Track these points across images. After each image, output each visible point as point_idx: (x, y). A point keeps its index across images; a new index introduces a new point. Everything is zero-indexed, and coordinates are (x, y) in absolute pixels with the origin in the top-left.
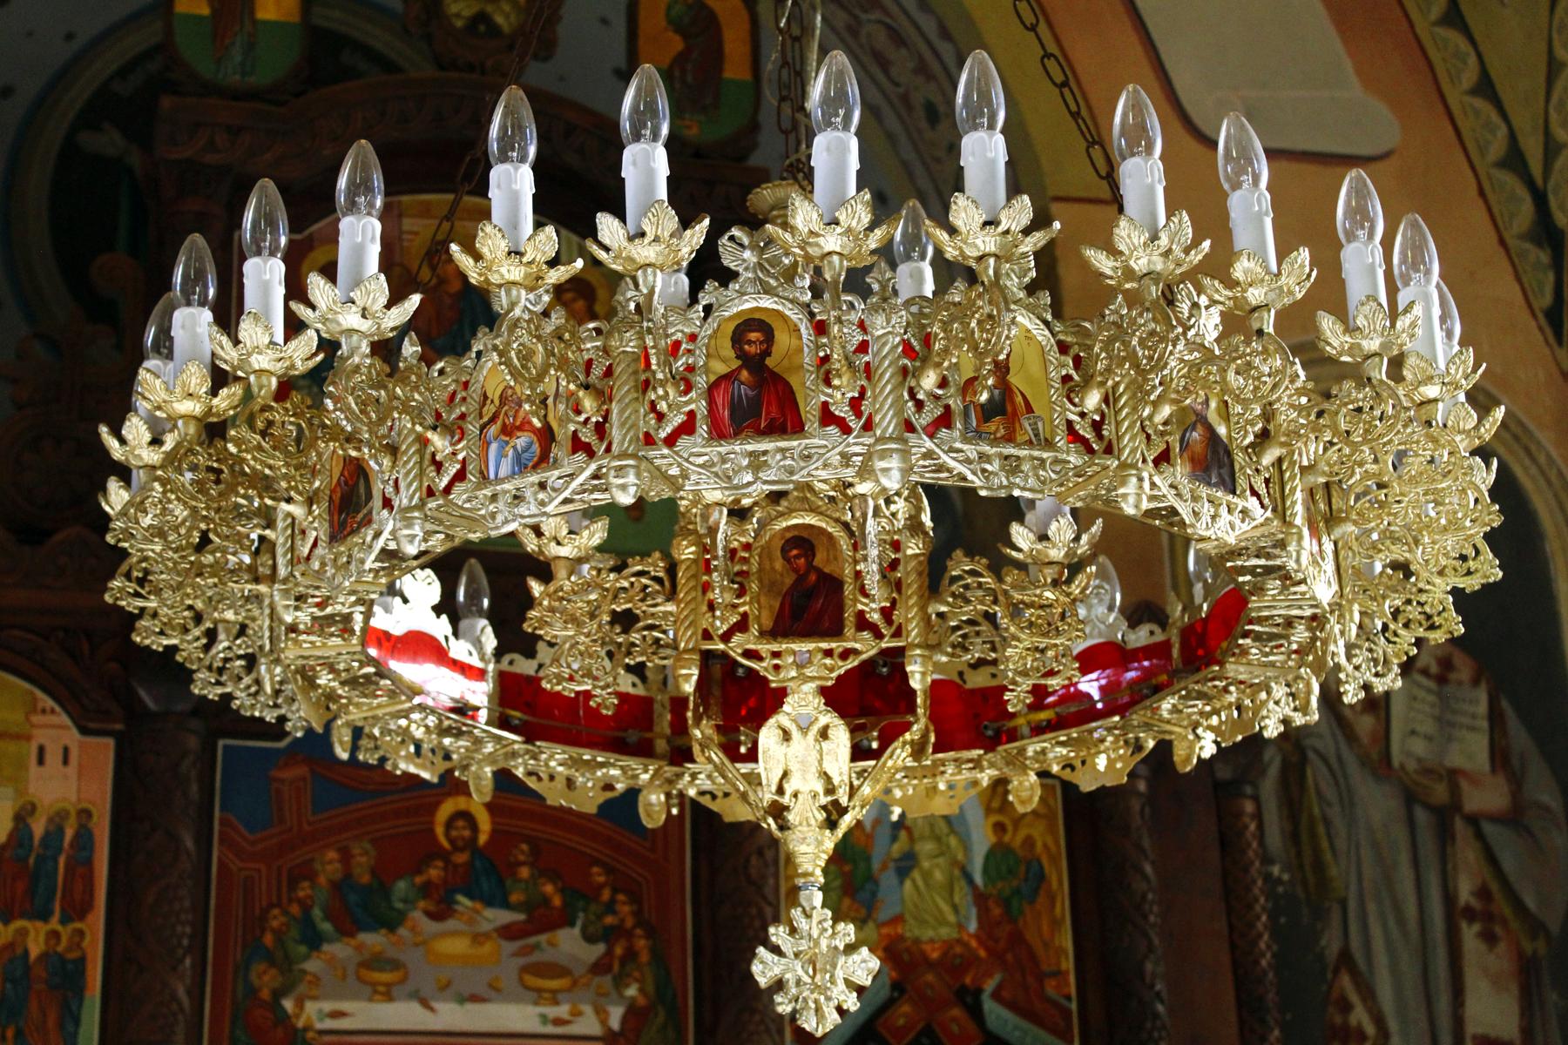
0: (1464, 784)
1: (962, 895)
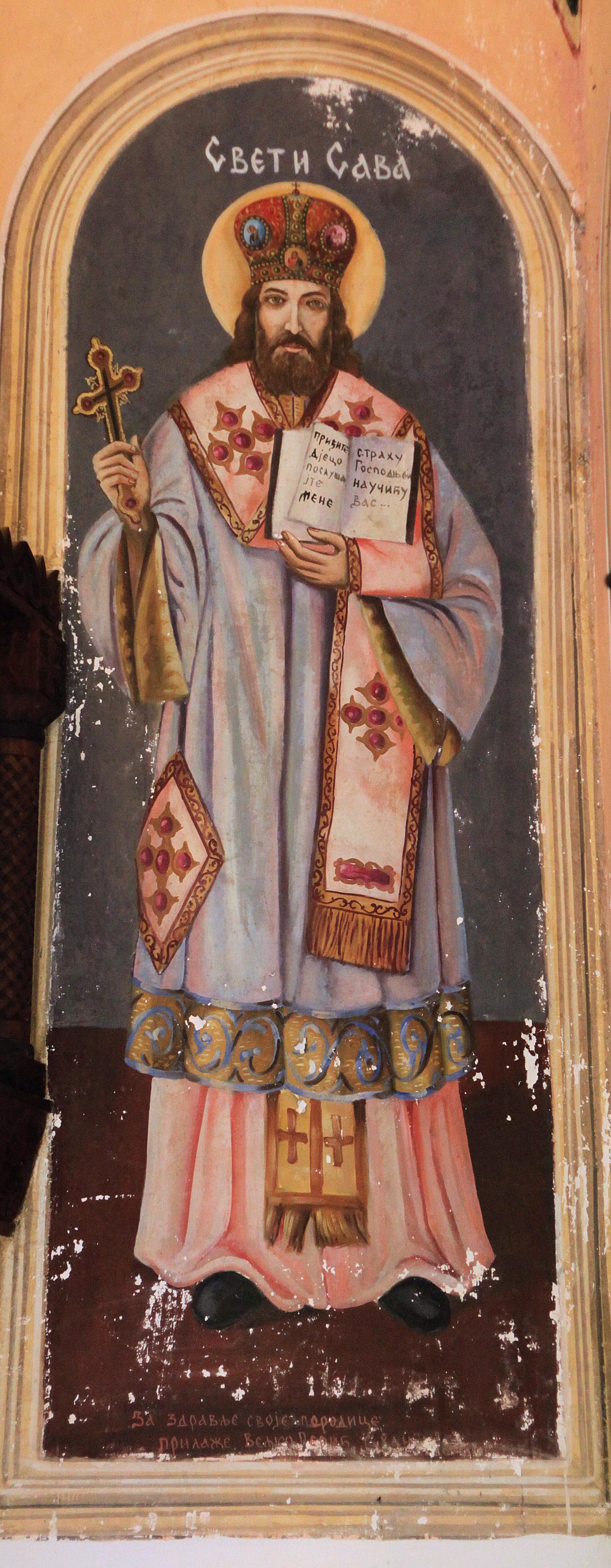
0: (366, 555)
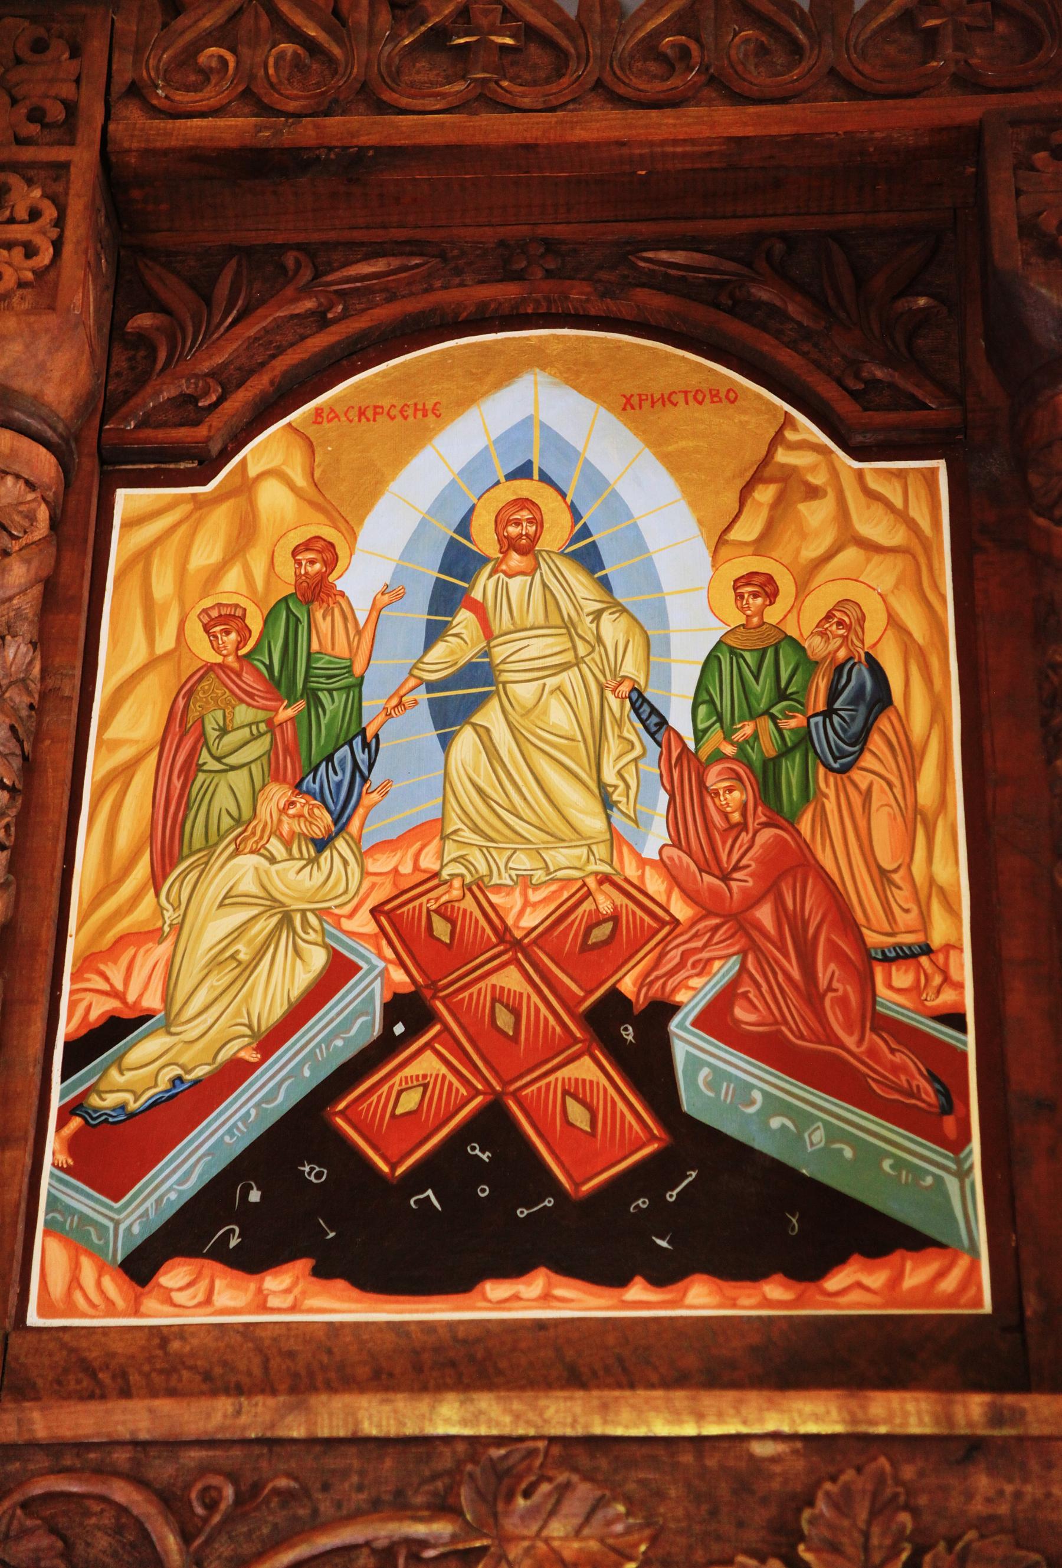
1: (631, 762)
